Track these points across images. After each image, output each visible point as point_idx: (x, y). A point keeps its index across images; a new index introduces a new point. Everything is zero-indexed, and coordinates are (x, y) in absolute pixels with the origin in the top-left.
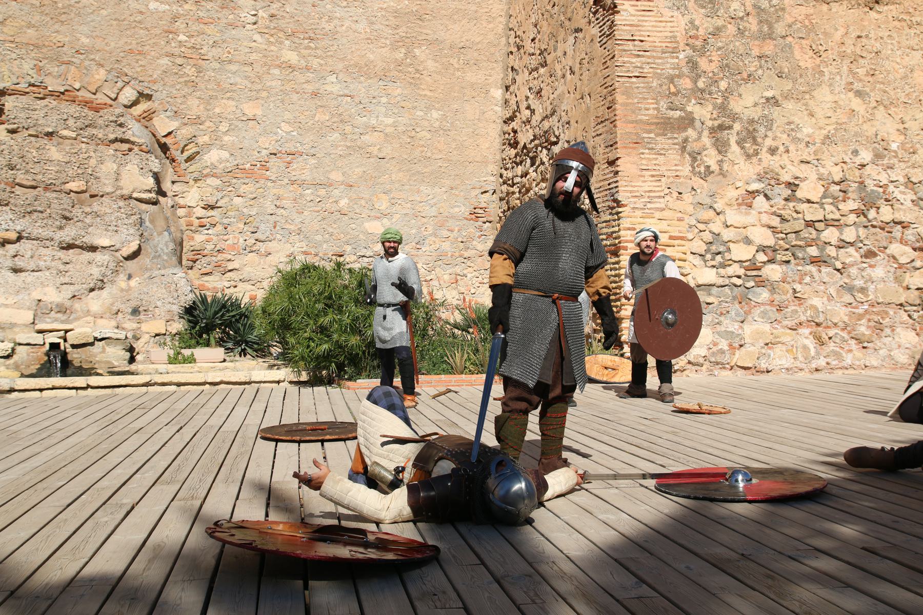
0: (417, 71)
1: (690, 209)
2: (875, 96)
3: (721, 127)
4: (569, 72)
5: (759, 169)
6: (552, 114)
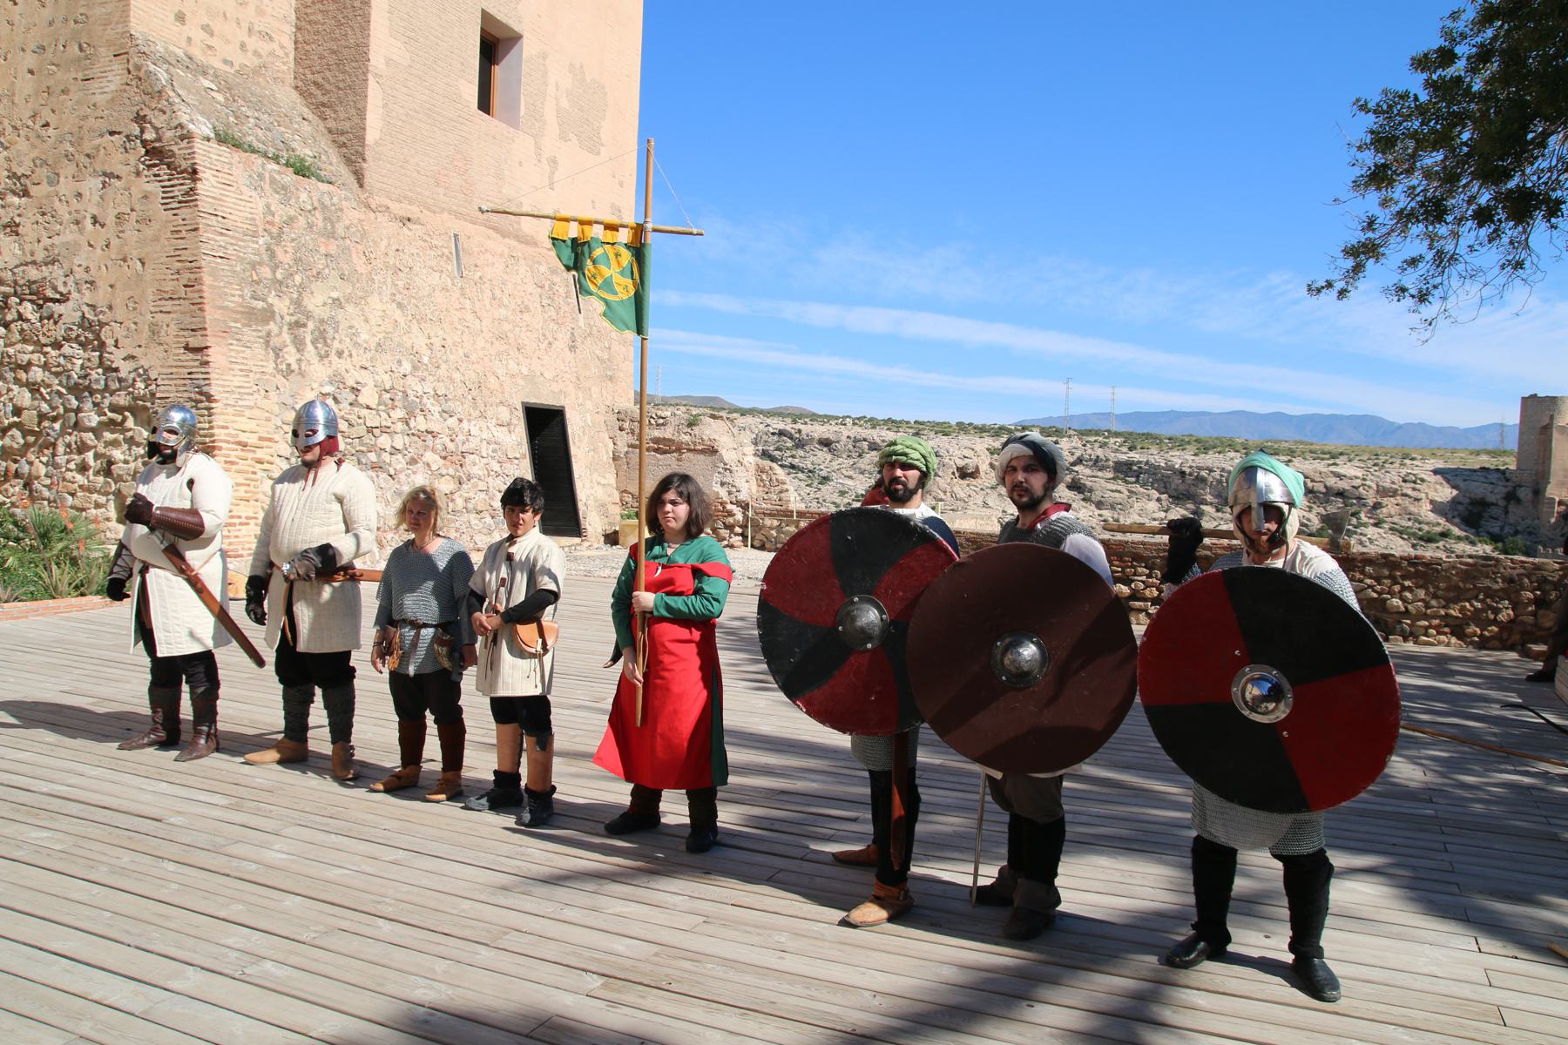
1: (276, 409)
2: (411, 310)
3: (298, 325)
4: (89, 221)
5: (330, 372)
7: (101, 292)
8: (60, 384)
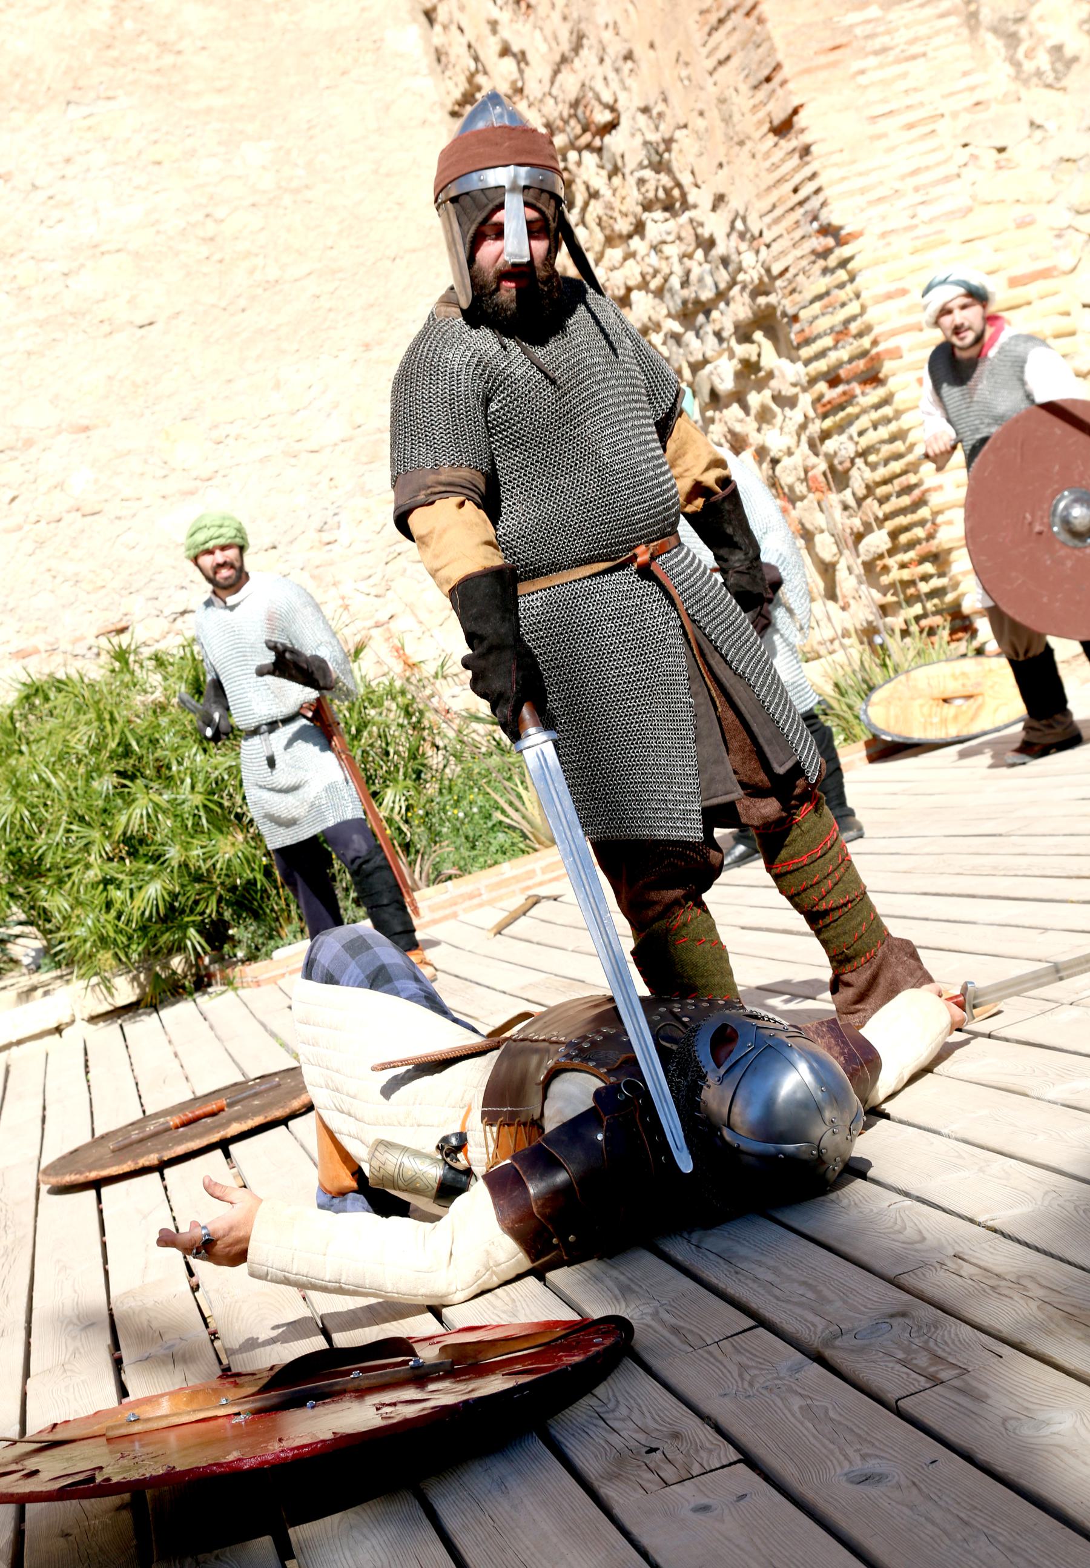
0: (164, 46)
6: (577, 48)
7: (644, 67)
8: (669, 315)
